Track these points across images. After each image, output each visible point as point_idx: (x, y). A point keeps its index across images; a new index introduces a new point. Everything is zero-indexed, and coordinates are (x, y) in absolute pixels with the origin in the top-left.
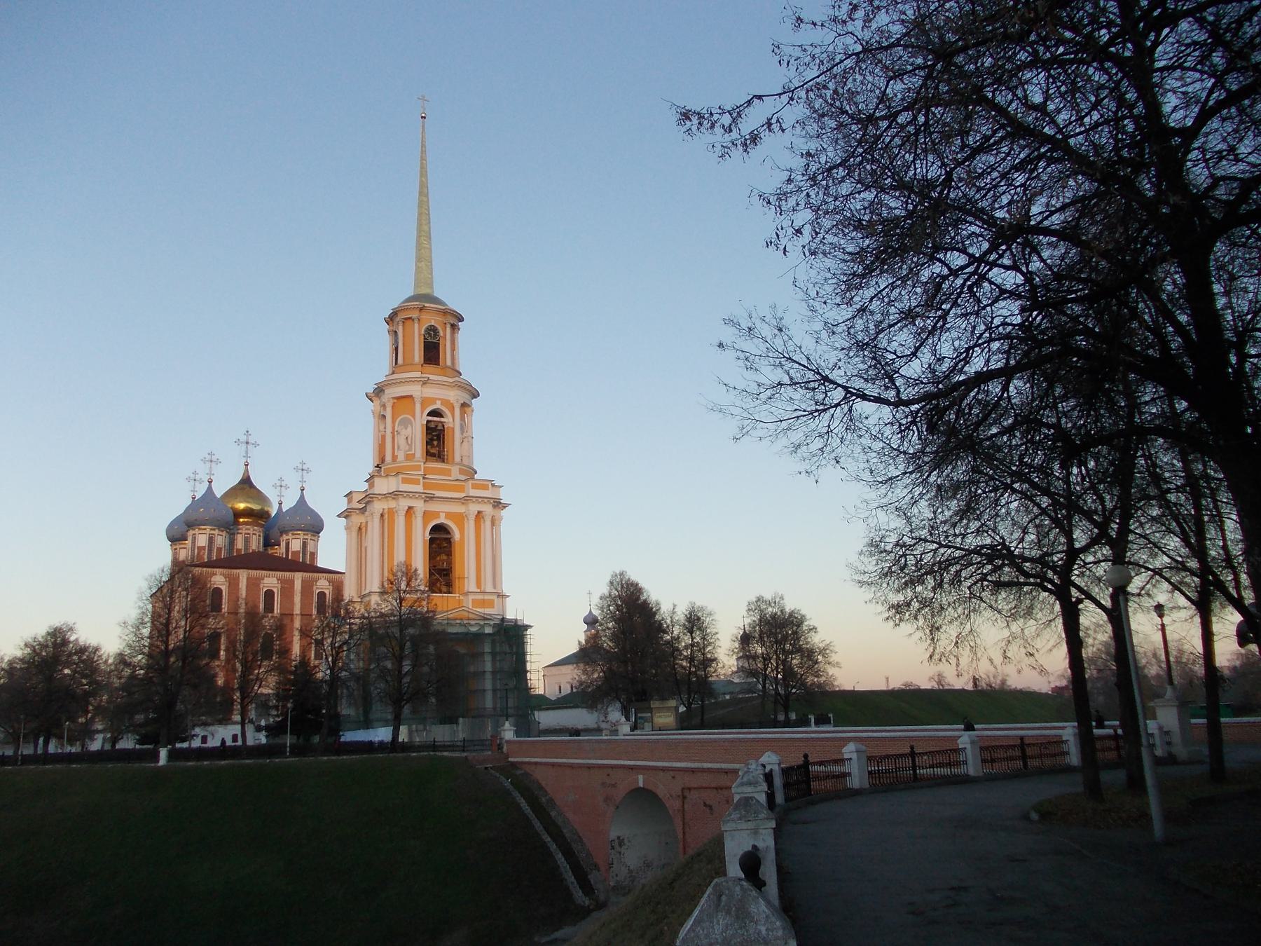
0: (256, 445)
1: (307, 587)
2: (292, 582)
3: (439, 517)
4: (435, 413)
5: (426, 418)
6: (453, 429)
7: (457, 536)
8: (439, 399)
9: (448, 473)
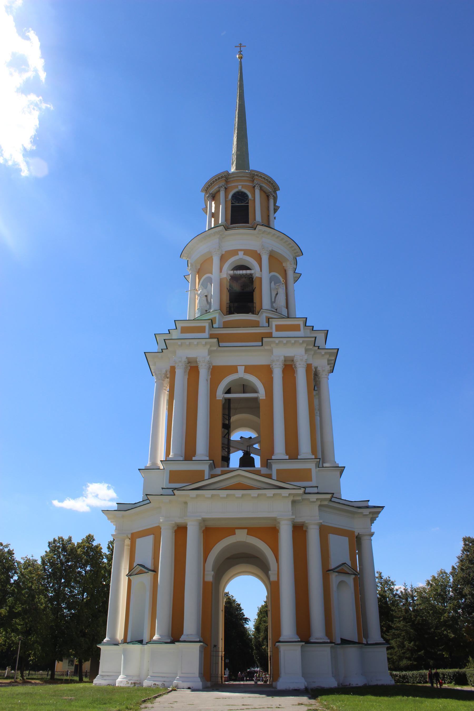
3: (237, 372)
5: (227, 272)
6: (261, 279)
8: (241, 250)
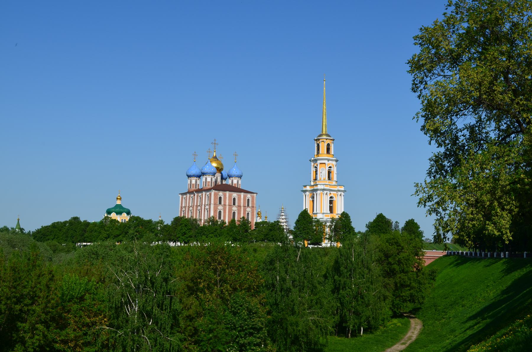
0: (218, 144)
1: (245, 197)
2: (240, 196)
4: (330, 167)
7: (334, 199)
9: (332, 183)
